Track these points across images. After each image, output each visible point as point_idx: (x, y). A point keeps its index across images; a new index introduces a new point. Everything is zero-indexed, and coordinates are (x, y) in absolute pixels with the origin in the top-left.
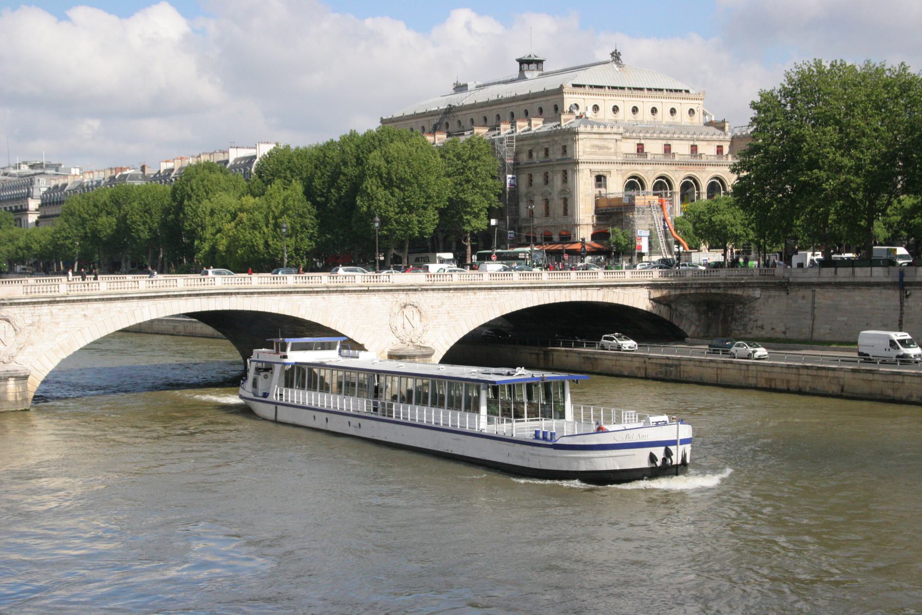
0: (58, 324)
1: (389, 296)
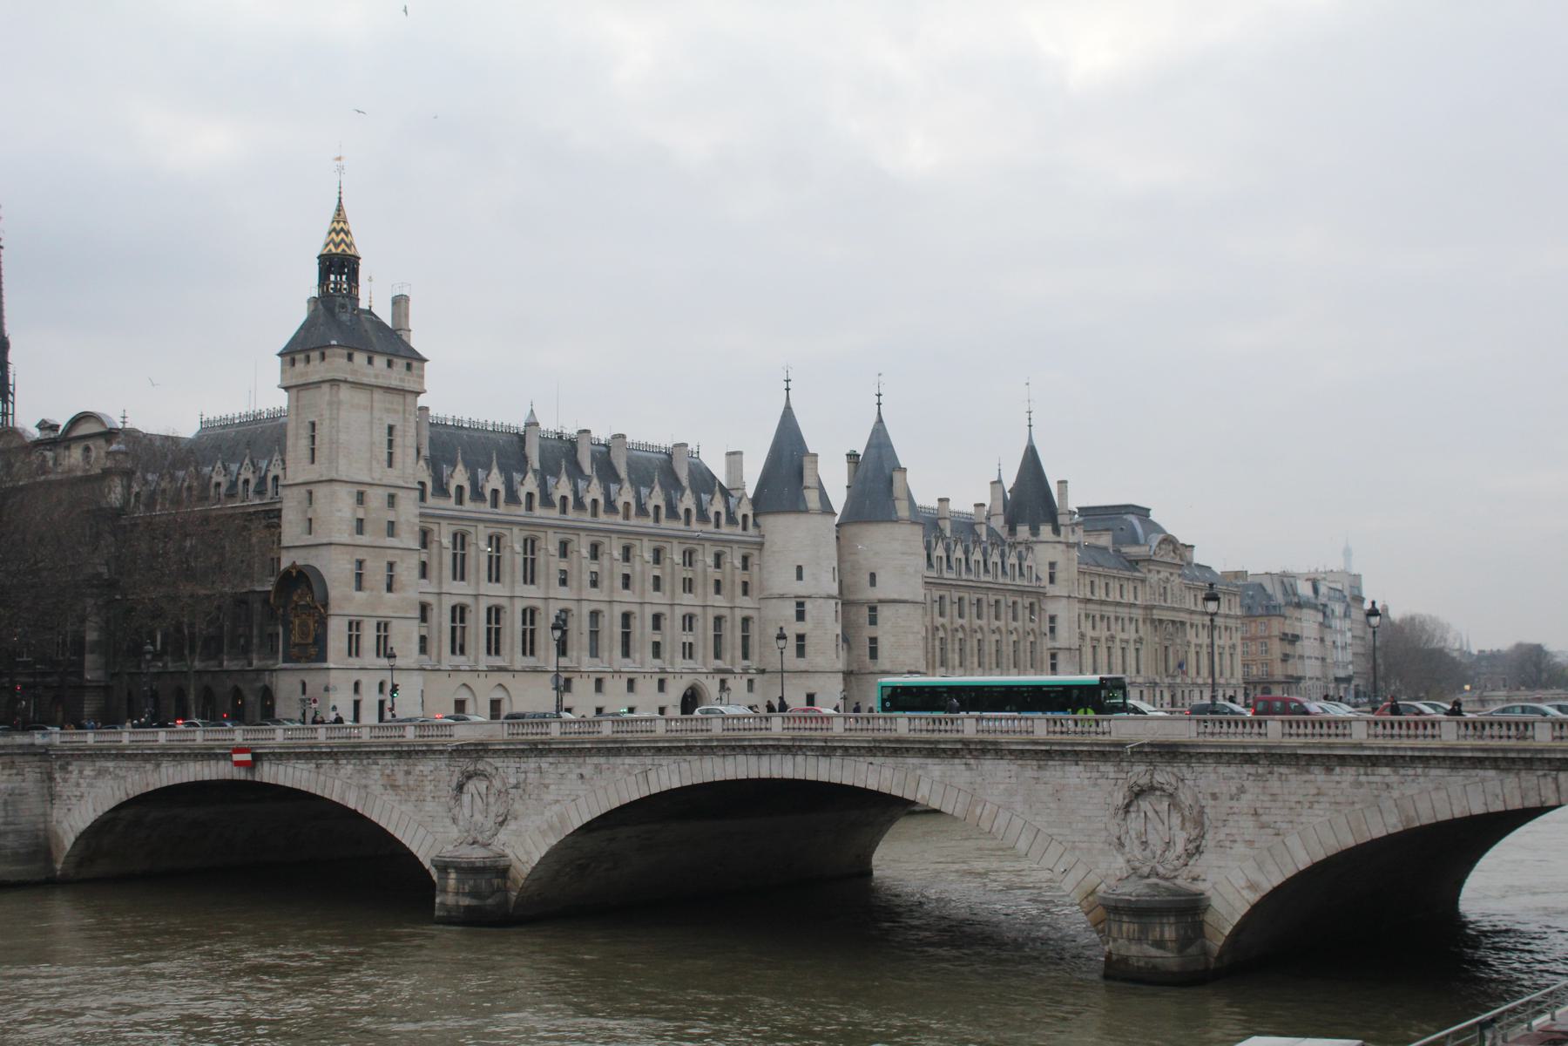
0: (547, 786)
1: (1109, 769)
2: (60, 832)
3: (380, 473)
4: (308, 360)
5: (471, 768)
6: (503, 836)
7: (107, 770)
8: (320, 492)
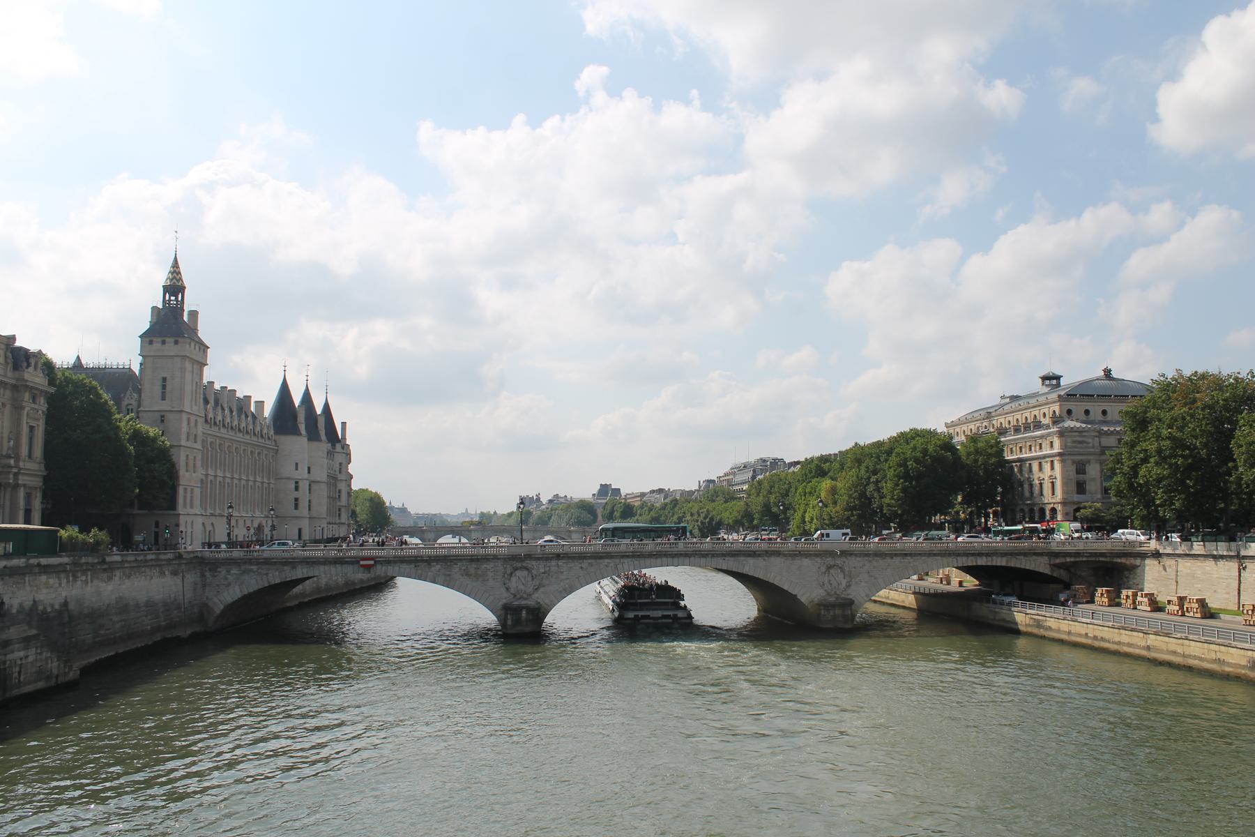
1: (818, 560)
2: (211, 604)
3: (195, 410)
4: (164, 343)
5: (519, 565)
6: (536, 595)
7: (251, 571)
8: (169, 416)
